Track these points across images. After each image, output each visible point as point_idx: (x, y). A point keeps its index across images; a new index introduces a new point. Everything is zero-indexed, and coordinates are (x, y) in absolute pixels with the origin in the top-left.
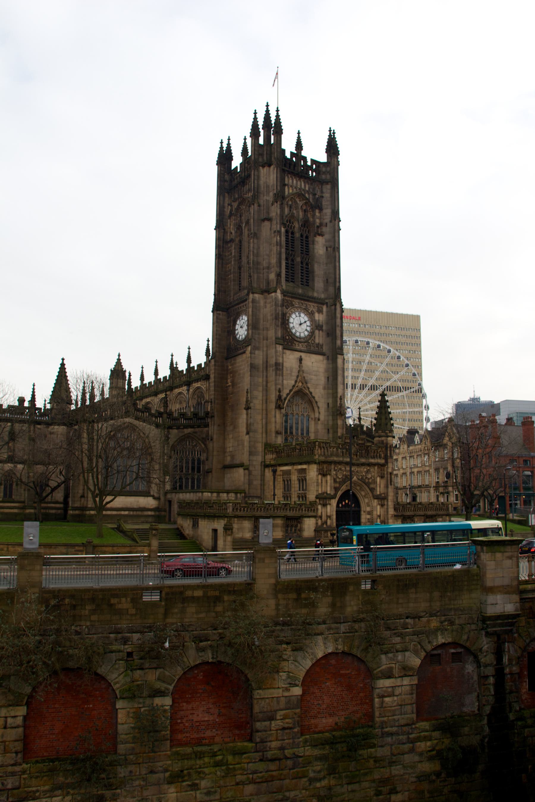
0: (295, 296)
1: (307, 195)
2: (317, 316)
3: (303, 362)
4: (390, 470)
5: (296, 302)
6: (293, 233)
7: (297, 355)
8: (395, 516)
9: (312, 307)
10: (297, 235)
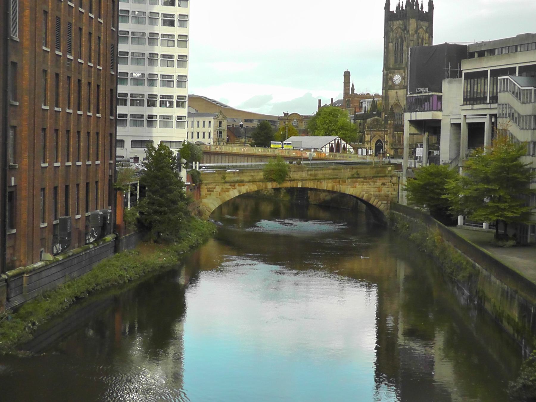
0: (395, 69)
1: (402, 26)
2: (404, 74)
3: (398, 93)
4: (389, 132)
5: (396, 71)
6: (398, 44)
7: (396, 91)
8: (391, 148)
9: (402, 71)
10: (399, 44)
